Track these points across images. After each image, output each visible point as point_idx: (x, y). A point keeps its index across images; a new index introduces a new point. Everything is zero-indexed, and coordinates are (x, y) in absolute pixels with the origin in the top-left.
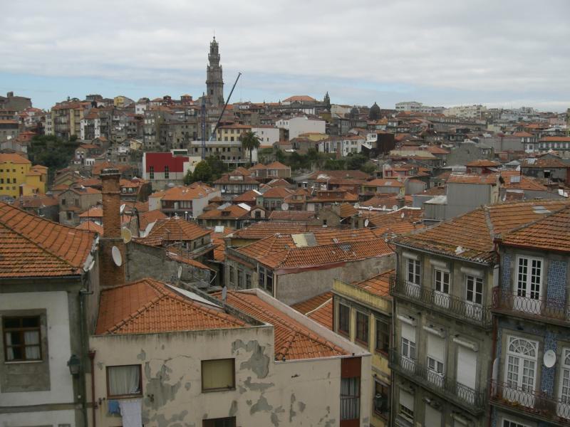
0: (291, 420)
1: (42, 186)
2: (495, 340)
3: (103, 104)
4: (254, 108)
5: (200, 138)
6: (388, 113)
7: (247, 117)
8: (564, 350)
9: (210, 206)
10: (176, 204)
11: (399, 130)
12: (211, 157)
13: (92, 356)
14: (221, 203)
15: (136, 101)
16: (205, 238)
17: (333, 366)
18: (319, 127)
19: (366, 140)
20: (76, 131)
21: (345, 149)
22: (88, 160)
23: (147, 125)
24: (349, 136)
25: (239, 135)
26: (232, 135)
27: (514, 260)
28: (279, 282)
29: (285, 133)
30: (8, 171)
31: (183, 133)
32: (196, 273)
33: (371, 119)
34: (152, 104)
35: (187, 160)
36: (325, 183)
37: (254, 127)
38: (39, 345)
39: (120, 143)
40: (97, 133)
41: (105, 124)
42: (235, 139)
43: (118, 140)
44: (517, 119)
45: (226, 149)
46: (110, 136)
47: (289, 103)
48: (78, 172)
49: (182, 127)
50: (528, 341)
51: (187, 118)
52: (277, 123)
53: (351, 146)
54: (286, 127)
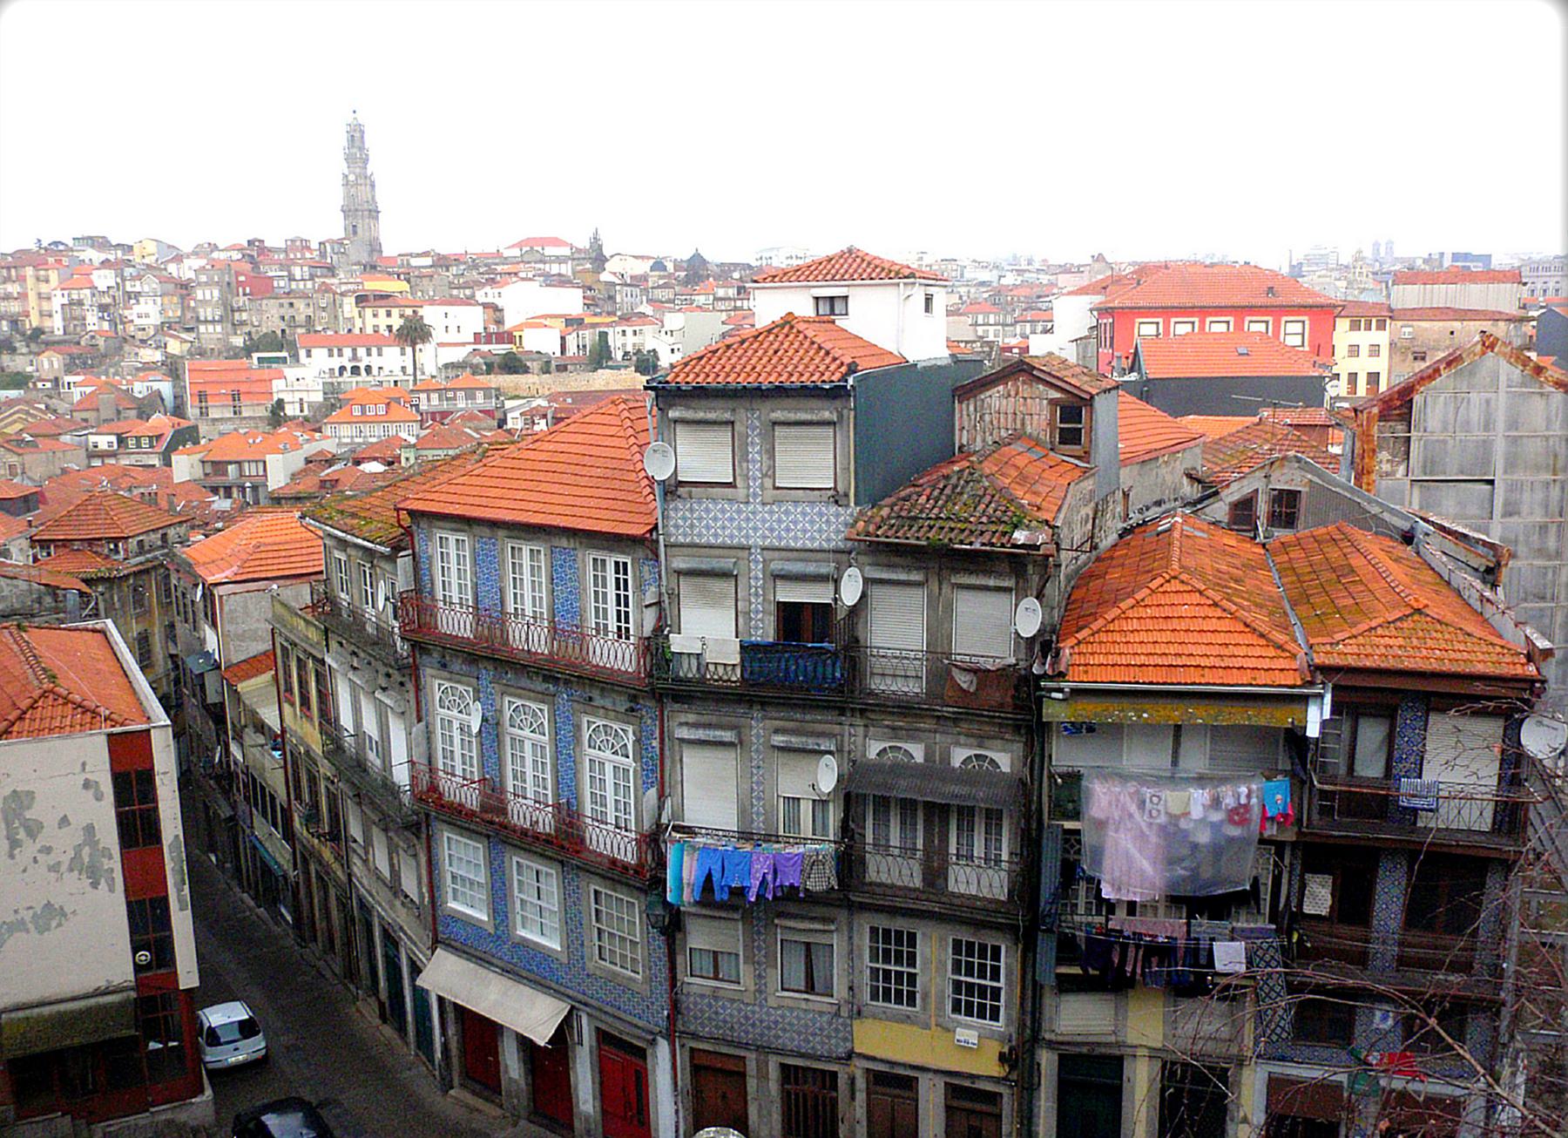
0: (12, 856)
2: (418, 689)
3: (112, 258)
4: (443, 262)
5: (319, 328)
6: (725, 271)
7: (425, 281)
8: (507, 699)
9: (304, 470)
11: (739, 303)
12: (342, 369)
14: (330, 462)
15: (187, 248)
16: (171, 532)
17: (90, 753)
18: (571, 301)
20: (41, 314)
21: (619, 344)
22: (68, 379)
23: (204, 302)
24: (628, 320)
25: (401, 322)
26: (389, 321)
27: (430, 538)
28: (226, 609)
29: (495, 310)
31: (283, 318)
32: (48, 600)
33: (687, 281)
34: (223, 256)
36: (545, 416)
37: (432, 302)
39: (143, 341)
40: (92, 318)
41: (107, 300)
42: (395, 329)
43: (140, 335)
44: (995, 279)
45: (374, 350)
46: (120, 327)
47: (516, 252)
48: (42, 406)
49: (281, 305)
50: (461, 688)
52: (480, 296)
53: (630, 342)
54: (500, 303)
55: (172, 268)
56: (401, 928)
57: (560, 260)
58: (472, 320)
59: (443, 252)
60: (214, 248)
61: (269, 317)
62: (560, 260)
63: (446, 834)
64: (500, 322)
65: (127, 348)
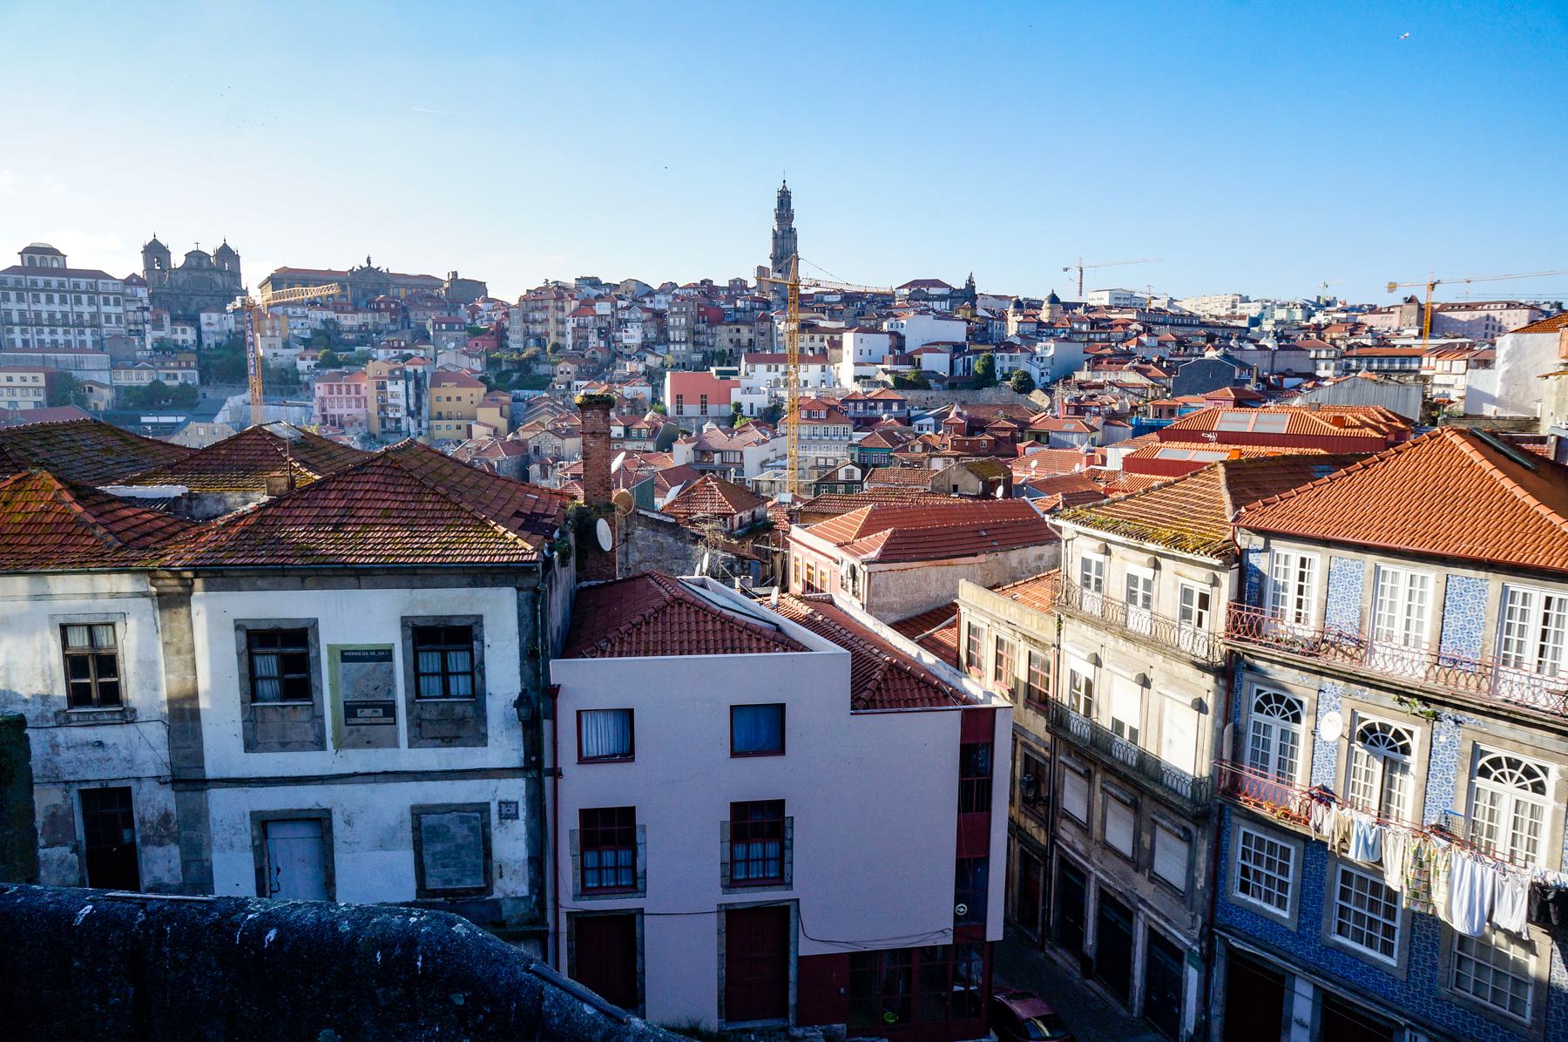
1: (502, 424)
4: (849, 298)
10: (717, 457)
12: (777, 381)
13: (553, 692)
15: (656, 287)
19: (1035, 353)
23: (675, 328)
26: (812, 345)
29: (898, 340)
30: (449, 399)
35: (737, 384)
38: (472, 674)
40: (593, 339)
41: (604, 324)
43: (626, 351)
47: (906, 291)
51: (738, 315)
53: (1007, 365)
54: (902, 332)
55: (647, 300)
56: (1143, 901)
57: (941, 298)
58: (882, 343)
59: (848, 289)
60: (674, 286)
61: (723, 338)
62: (941, 298)
63: (1243, 829)
64: (901, 347)
65: (618, 361)
